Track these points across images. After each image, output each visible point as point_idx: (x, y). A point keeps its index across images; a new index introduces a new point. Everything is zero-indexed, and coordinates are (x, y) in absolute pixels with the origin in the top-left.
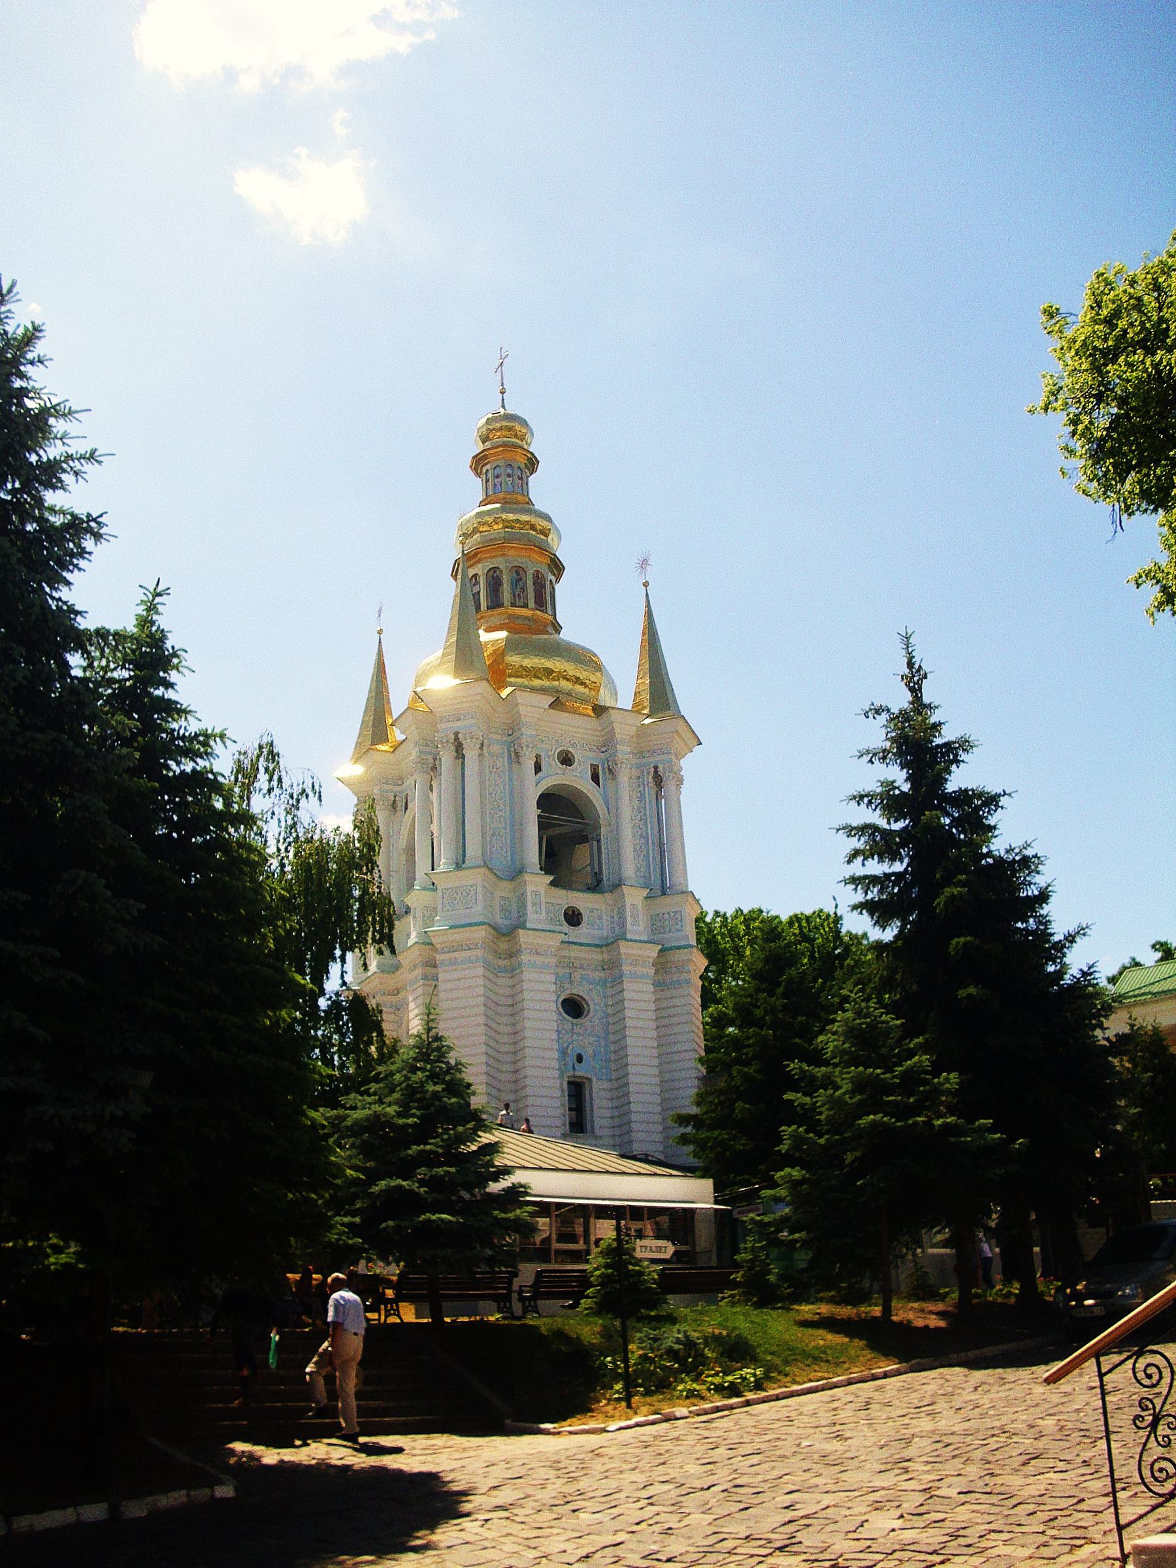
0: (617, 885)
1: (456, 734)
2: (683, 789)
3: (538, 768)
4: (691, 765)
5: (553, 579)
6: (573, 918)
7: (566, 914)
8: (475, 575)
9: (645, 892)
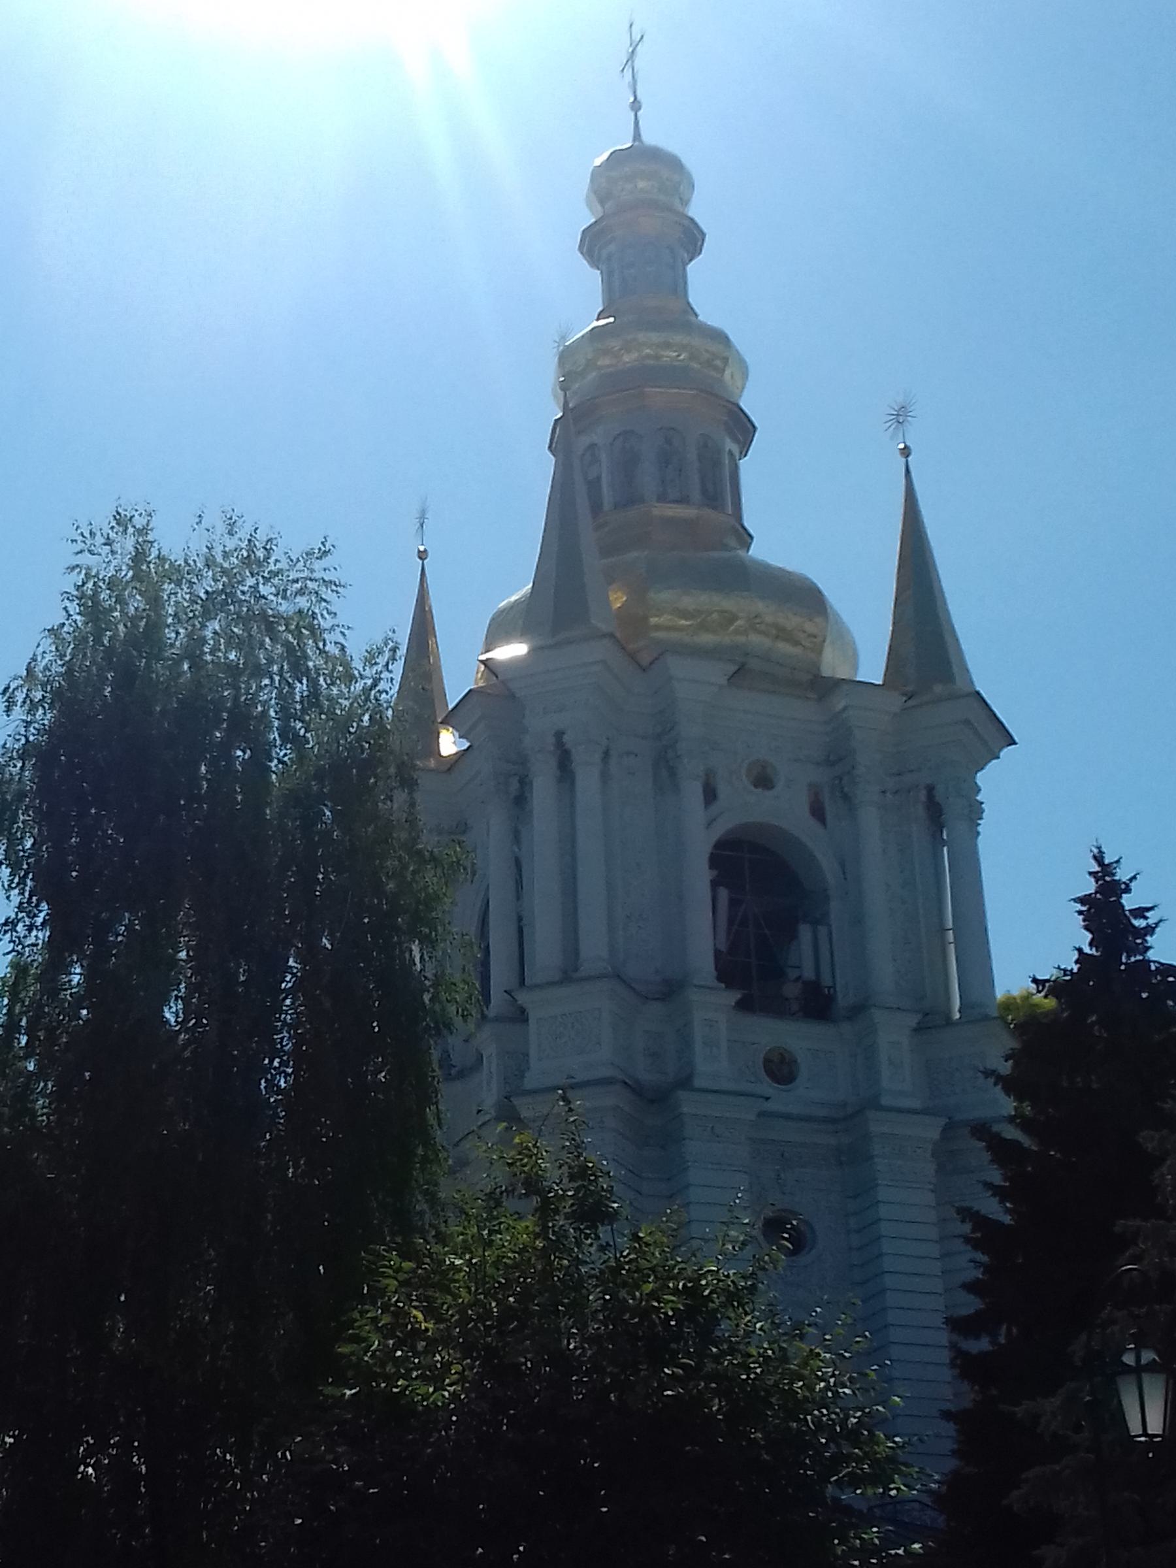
0: (859, 1010)
1: (559, 735)
2: (984, 826)
3: (710, 795)
4: (994, 782)
5: (736, 449)
6: (781, 1069)
7: (767, 1062)
8: (593, 446)
9: (913, 1020)
